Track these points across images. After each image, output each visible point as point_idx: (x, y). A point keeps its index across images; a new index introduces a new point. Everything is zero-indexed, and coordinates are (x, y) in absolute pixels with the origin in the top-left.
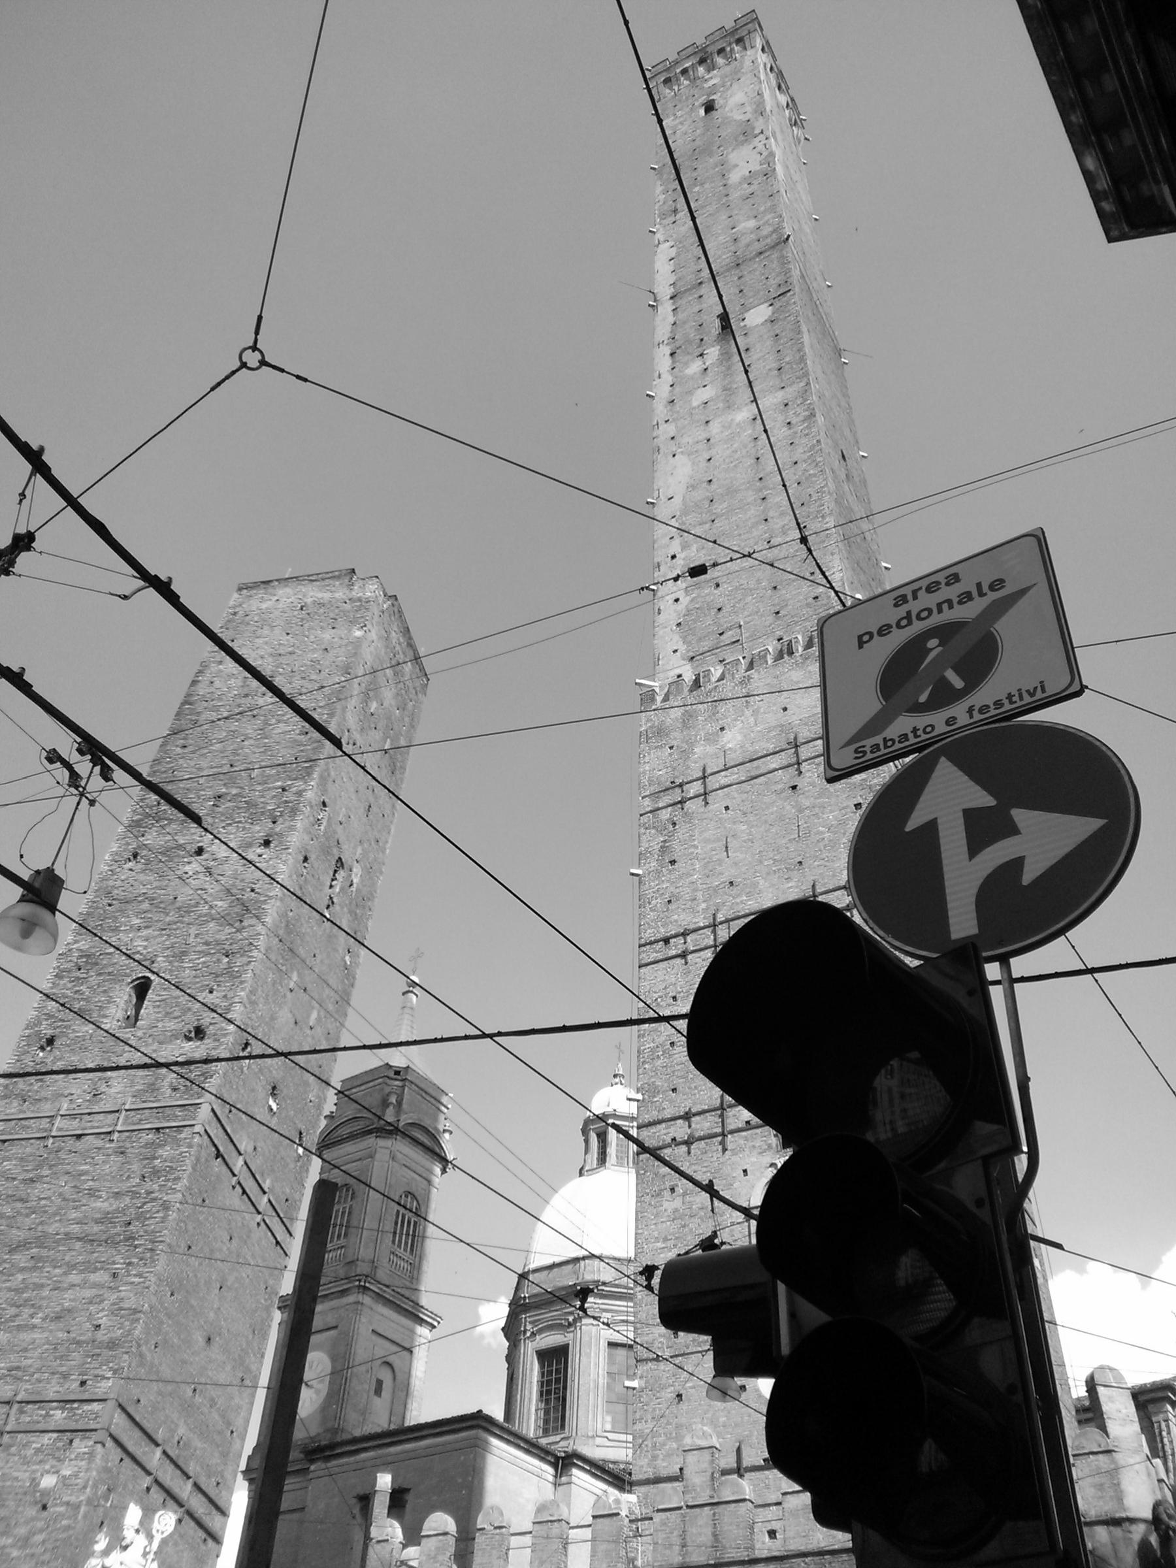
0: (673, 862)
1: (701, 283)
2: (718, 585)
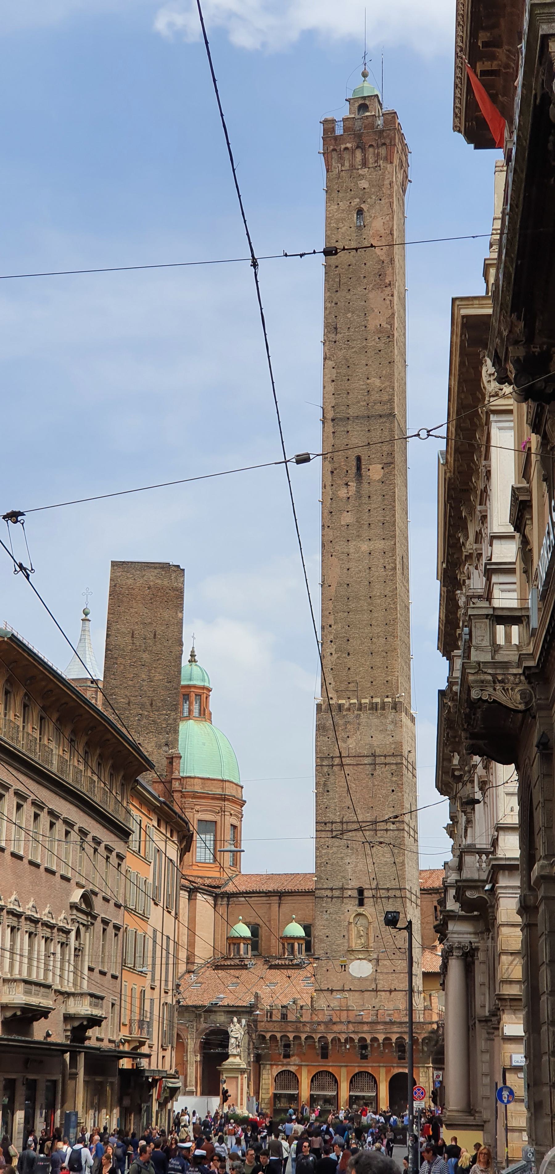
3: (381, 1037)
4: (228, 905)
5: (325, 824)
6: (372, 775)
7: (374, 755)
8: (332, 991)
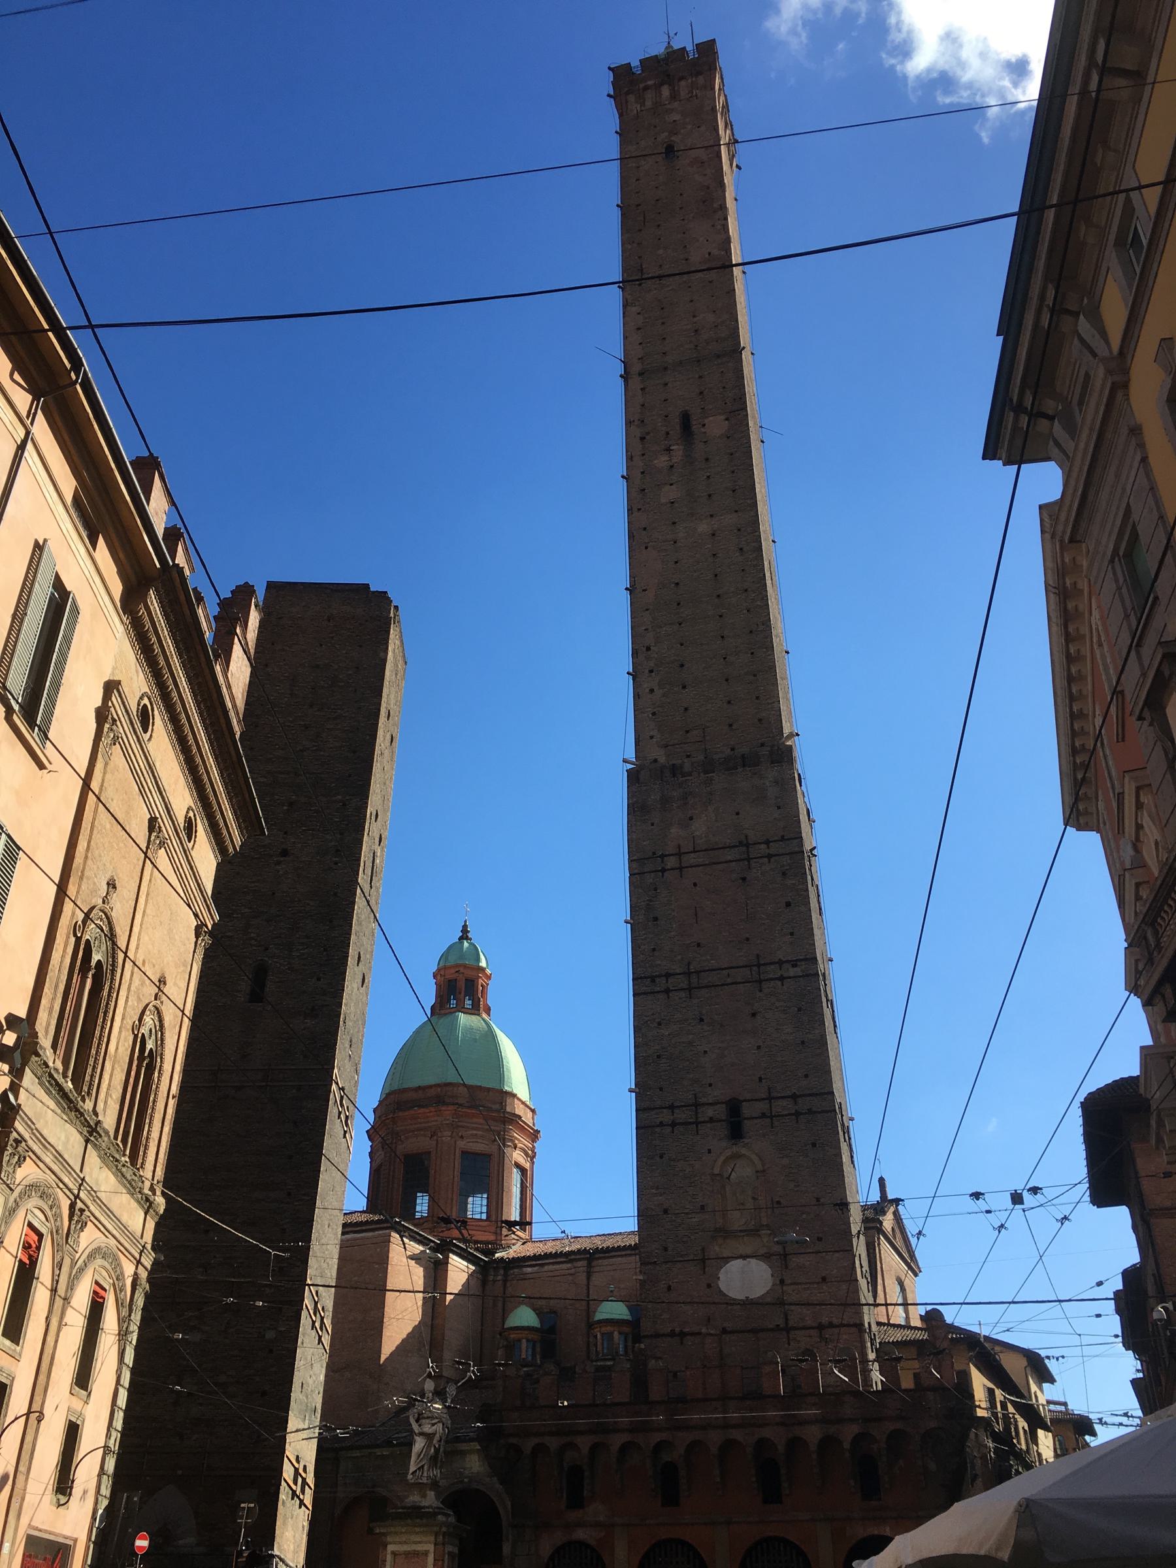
0: (656, 919)
1: (666, 369)
2: (684, 687)
3: (813, 1434)
4: (505, 1281)
5: (653, 981)
6: (744, 879)
7: (745, 844)
8: (682, 1335)
